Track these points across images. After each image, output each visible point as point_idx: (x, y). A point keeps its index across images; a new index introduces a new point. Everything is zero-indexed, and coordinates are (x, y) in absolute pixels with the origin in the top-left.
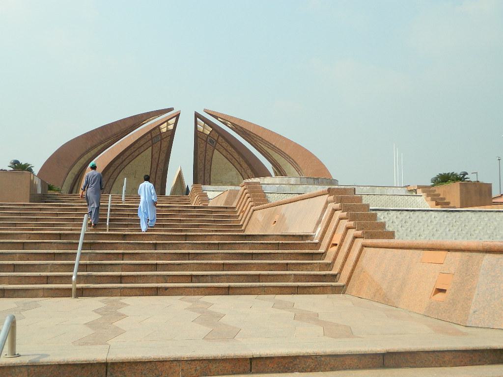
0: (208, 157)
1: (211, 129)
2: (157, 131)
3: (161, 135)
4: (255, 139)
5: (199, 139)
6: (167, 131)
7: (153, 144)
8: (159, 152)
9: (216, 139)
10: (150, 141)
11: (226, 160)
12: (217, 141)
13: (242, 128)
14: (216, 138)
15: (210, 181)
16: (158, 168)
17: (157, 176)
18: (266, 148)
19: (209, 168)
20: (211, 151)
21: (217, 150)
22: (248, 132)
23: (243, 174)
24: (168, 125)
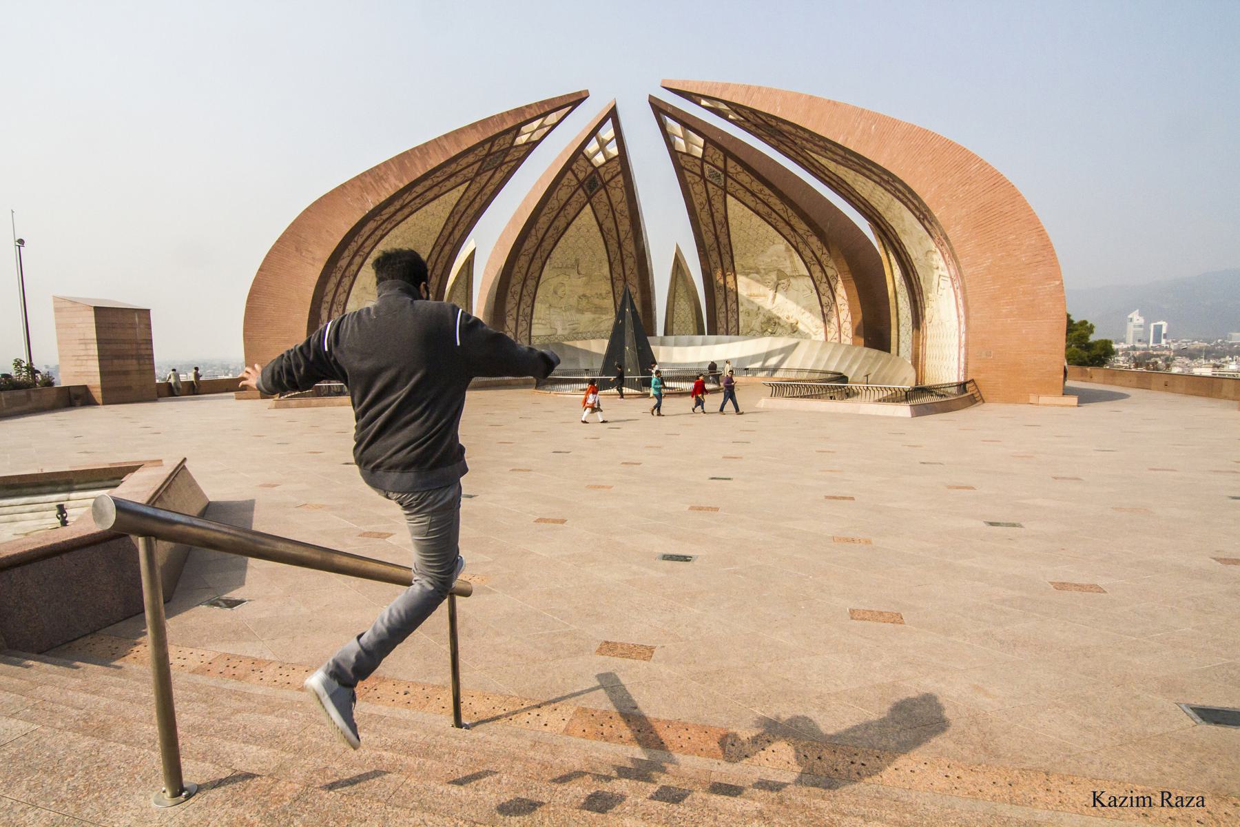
0: (719, 217)
1: (701, 141)
2: (582, 162)
4: (798, 141)
5: (687, 174)
6: (608, 161)
7: (589, 200)
8: (611, 214)
10: (581, 191)
12: (725, 172)
13: (753, 111)
17: (627, 268)
18: (832, 166)
19: (726, 241)
20: (721, 199)
22: (774, 123)
23: (801, 246)
24: (603, 145)
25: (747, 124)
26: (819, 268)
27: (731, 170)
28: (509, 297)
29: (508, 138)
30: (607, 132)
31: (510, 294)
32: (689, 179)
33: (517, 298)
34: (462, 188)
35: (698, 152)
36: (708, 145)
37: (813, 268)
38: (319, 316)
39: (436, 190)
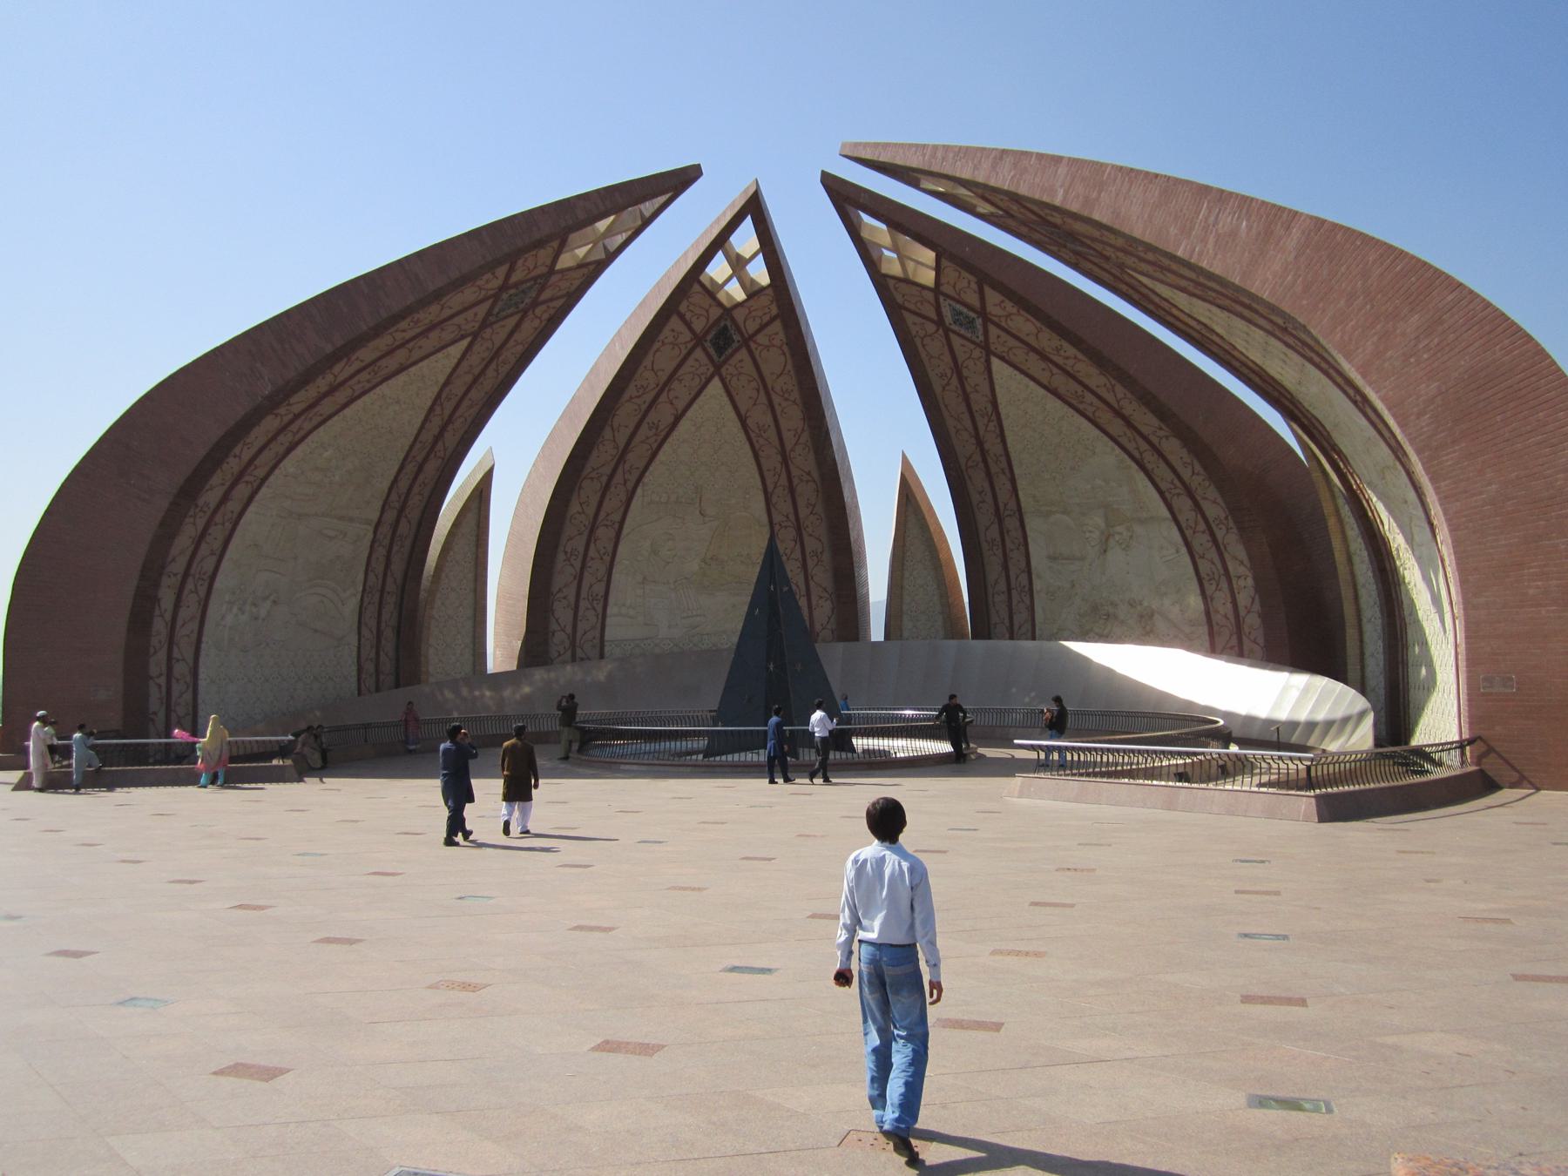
0: (980, 401)
1: (929, 256)
3: (733, 320)
4: (1109, 252)
8: (763, 398)
9: (976, 302)
10: (699, 353)
11: (1059, 403)
12: (983, 313)
13: (1015, 198)
16: (795, 472)
17: (801, 502)
18: (1181, 299)
19: (998, 449)
20: (981, 366)
21: (1002, 359)
22: (1057, 219)
25: (1010, 222)
26: (1190, 502)
27: (992, 309)
29: (544, 254)
30: (745, 240)
31: (561, 557)
32: (914, 330)
33: (578, 565)
34: (456, 351)
35: (928, 277)
36: (944, 263)
37: (1176, 503)
38: (155, 600)
39: (401, 355)
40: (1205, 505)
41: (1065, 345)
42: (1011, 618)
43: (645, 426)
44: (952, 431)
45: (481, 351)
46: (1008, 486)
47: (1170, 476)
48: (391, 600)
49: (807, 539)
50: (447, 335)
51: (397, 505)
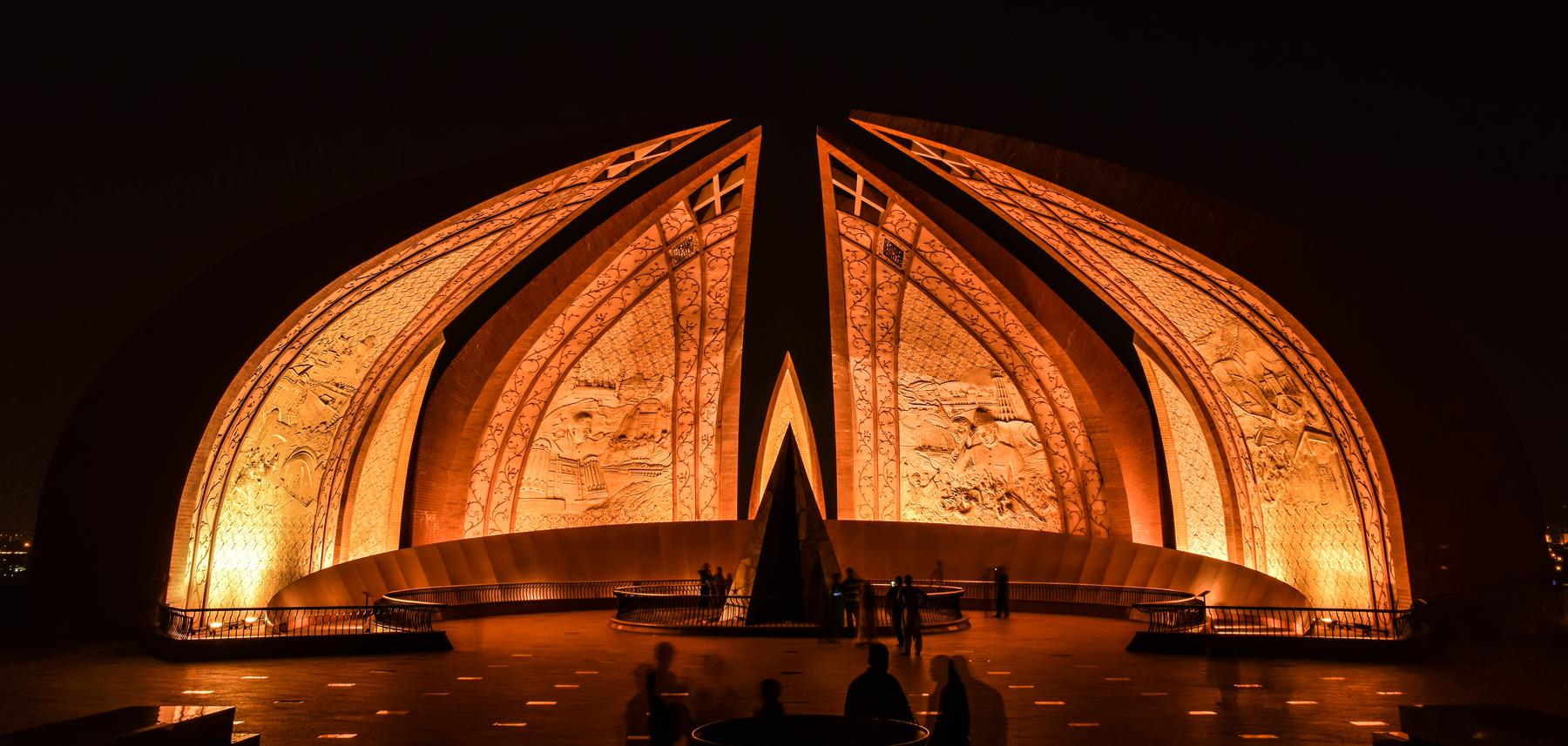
3: (700, 237)
4: (1072, 218)
9: (909, 240)
14: (908, 236)
15: (897, 408)
16: (706, 365)
20: (895, 290)
21: (916, 283)
28: (486, 437)
31: (488, 431)
33: (500, 439)
40: (1064, 412)
41: (975, 278)
42: (876, 500)
43: (593, 316)
44: (850, 338)
45: (503, 243)
46: (890, 387)
47: (1036, 387)
48: (344, 466)
49: (701, 424)
50: (490, 227)
51: (374, 376)
